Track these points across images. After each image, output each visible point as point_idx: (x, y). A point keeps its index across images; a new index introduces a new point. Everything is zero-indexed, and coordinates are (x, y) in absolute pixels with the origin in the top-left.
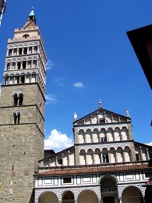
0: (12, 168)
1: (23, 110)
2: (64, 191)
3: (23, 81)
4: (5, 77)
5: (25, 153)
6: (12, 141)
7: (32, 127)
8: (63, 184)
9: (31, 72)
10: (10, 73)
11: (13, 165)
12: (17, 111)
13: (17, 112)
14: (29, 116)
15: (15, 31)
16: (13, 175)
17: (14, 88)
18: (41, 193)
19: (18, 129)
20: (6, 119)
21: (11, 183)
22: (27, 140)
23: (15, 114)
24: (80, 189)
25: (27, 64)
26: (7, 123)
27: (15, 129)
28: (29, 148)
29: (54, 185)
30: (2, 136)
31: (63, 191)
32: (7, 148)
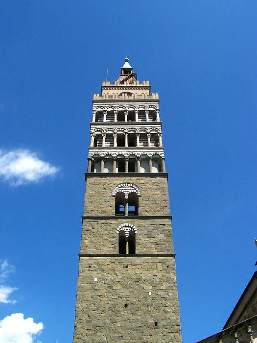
1: (142, 226)
3: (133, 168)
4: (93, 159)
5: (156, 324)
6: (123, 294)
7: (167, 264)
9: (148, 153)
10: (104, 153)
12: (128, 227)
13: (127, 231)
14: (157, 239)
15: (104, 85)
19: (133, 267)
20: (102, 243)
22: (159, 293)
26: (105, 251)
27: (127, 267)
30: (96, 280)
32: (111, 309)
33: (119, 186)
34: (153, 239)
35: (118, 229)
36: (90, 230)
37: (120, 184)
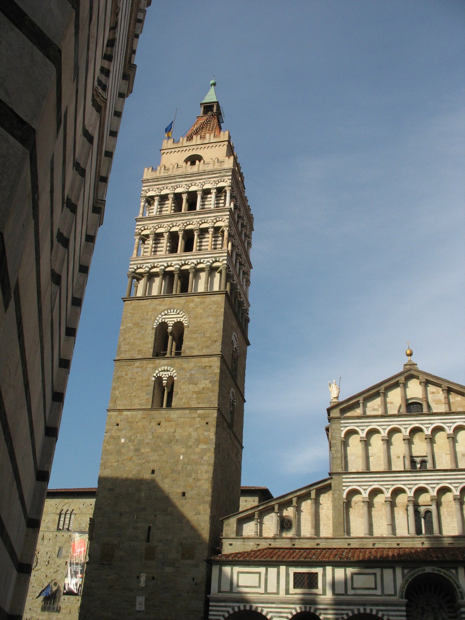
0: (146, 535)
1: (183, 369)
2: (294, 613)
7: (207, 420)
8: (292, 590)
9: (206, 260)
10: (148, 265)
11: (150, 528)
13: (165, 376)
16: (150, 554)
17: (160, 305)
18: (226, 615)
20: (134, 394)
21: (143, 579)
22: (193, 457)
23: (159, 380)
24: (343, 610)
25: (196, 237)
27: (159, 424)
28: (198, 480)
29: (266, 592)
31: (291, 613)
33: (163, 314)
34: (194, 385)
35: (155, 375)
36: (122, 377)
37: (163, 311)
